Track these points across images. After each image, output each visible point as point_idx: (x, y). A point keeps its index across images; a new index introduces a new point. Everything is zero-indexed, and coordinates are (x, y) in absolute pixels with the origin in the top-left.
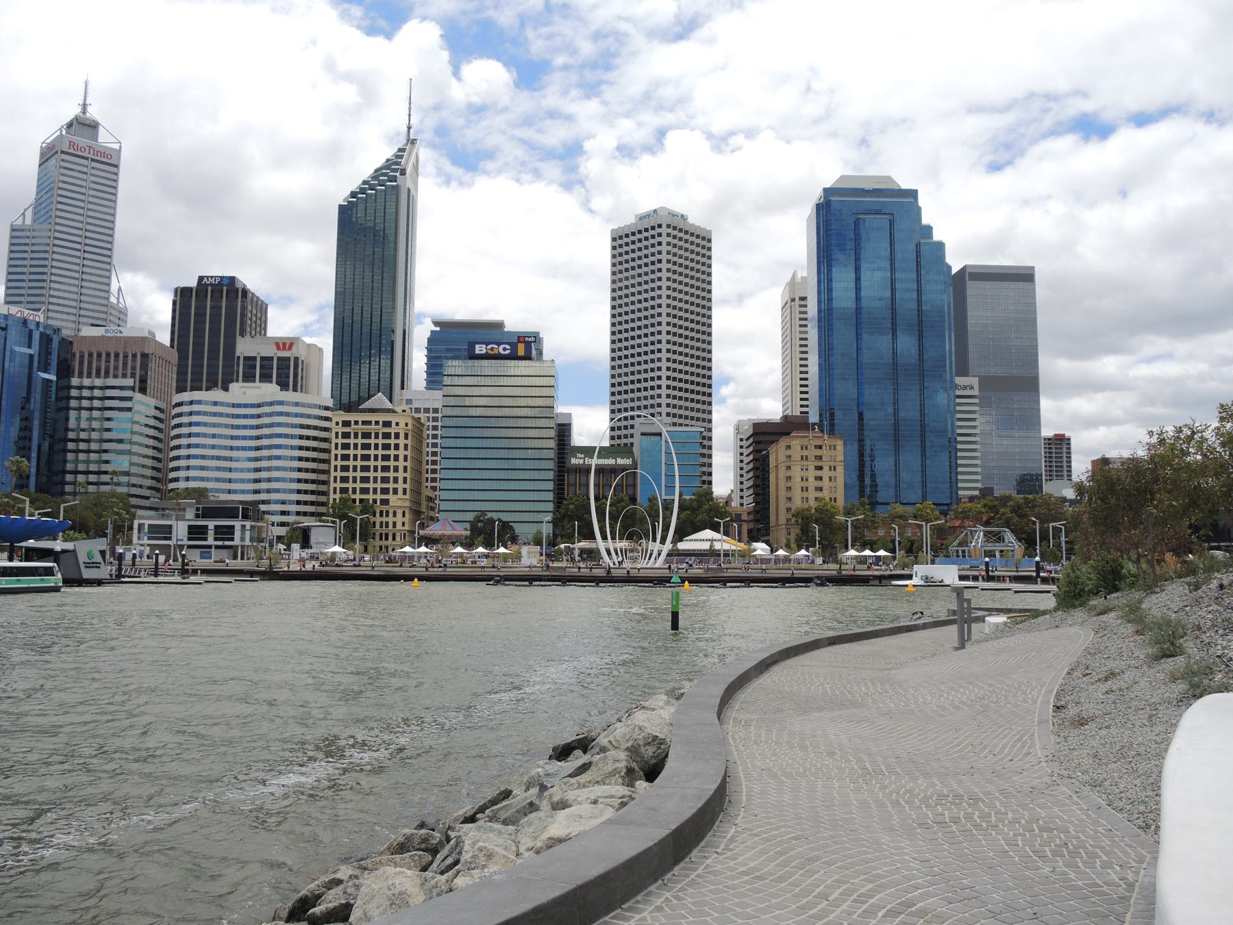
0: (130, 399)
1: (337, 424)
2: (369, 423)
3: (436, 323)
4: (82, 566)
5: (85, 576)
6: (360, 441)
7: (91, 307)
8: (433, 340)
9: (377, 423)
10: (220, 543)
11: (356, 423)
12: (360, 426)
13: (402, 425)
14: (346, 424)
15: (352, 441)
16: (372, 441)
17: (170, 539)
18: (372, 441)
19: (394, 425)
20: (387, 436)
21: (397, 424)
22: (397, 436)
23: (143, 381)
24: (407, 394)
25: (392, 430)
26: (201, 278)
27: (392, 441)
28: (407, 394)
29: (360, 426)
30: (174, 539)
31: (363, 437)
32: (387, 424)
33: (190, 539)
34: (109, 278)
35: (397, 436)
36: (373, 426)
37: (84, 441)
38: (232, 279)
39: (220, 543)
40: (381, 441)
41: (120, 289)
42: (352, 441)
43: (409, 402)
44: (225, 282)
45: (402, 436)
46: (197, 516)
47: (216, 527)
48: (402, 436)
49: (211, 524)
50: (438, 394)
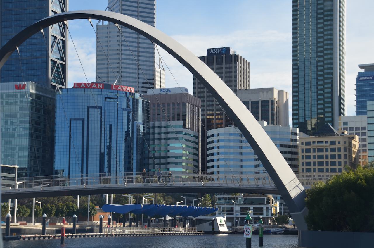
0: (180, 132)
1: (302, 144)
2: (322, 142)
3: (361, 67)
4: (219, 225)
5: (220, 230)
6: (317, 154)
7: (131, 62)
8: (360, 81)
9: (326, 142)
10: (256, 216)
11: (314, 142)
12: (316, 144)
13: (342, 143)
14: (308, 143)
15: (312, 154)
16: (324, 154)
17: (233, 214)
18: (324, 154)
19: (337, 143)
20: (333, 150)
21: (339, 143)
22: (339, 150)
23: (184, 120)
24: (342, 119)
25: (336, 146)
26: (209, 50)
27: (337, 153)
28: (342, 119)
29: (316, 144)
30: (235, 214)
31: (318, 152)
32: (333, 143)
33: (241, 214)
34: (154, 53)
35: (339, 150)
36: (324, 144)
37: (164, 158)
38: (228, 49)
39: (256, 216)
40: (329, 153)
41: (160, 60)
42: (312, 154)
43: (345, 123)
44: (224, 51)
45: (342, 150)
46: (244, 203)
47: (254, 208)
48: (342, 150)
49: (252, 207)
50: (364, 117)
